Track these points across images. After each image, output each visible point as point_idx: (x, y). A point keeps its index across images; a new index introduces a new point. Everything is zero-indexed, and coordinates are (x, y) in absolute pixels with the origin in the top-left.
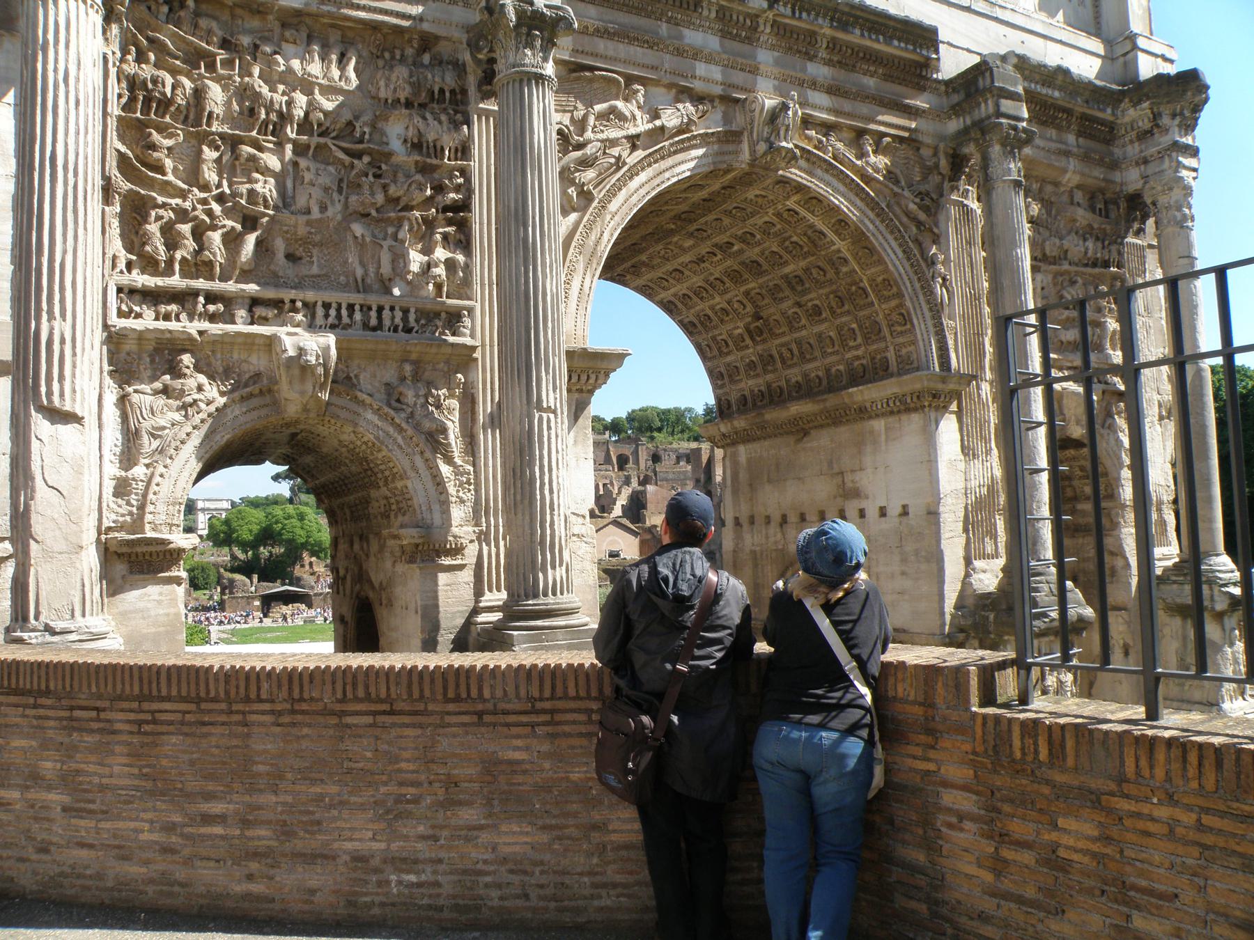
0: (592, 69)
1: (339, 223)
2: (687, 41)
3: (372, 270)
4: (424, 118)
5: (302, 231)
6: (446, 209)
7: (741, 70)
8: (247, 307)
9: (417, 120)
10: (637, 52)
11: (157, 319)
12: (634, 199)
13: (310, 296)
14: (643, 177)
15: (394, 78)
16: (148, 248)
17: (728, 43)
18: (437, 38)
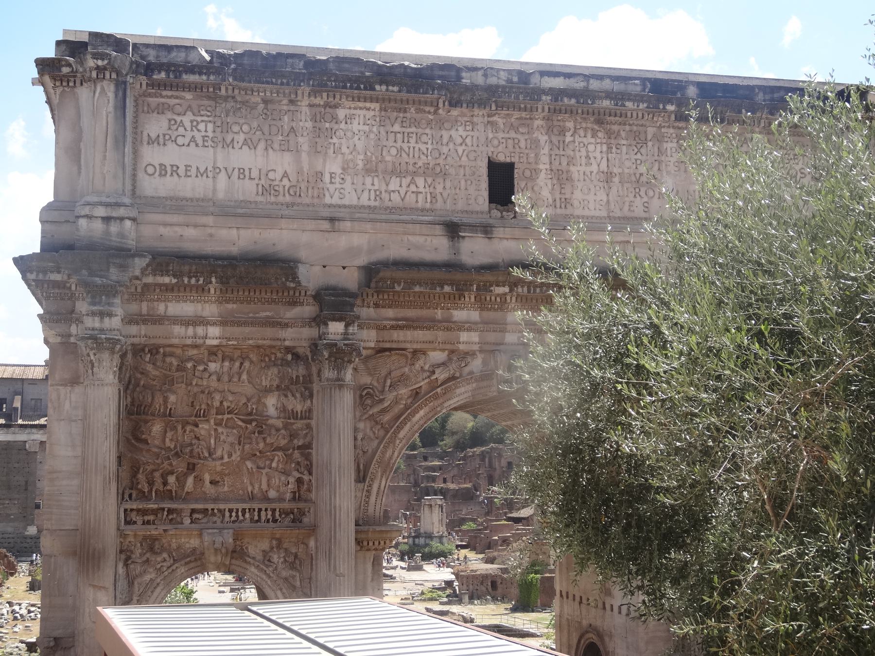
0: (390, 350)
1: (239, 462)
2: (455, 319)
3: (257, 486)
4: (286, 396)
5: (219, 469)
6: (299, 448)
7: (494, 331)
8: (189, 515)
9: (282, 398)
10: (420, 334)
11: (144, 524)
12: (416, 427)
13: (222, 506)
14: (422, 413)
15: (270, 374)
16: (140, 486)
17: (486, 314)
18: (294, 347)
